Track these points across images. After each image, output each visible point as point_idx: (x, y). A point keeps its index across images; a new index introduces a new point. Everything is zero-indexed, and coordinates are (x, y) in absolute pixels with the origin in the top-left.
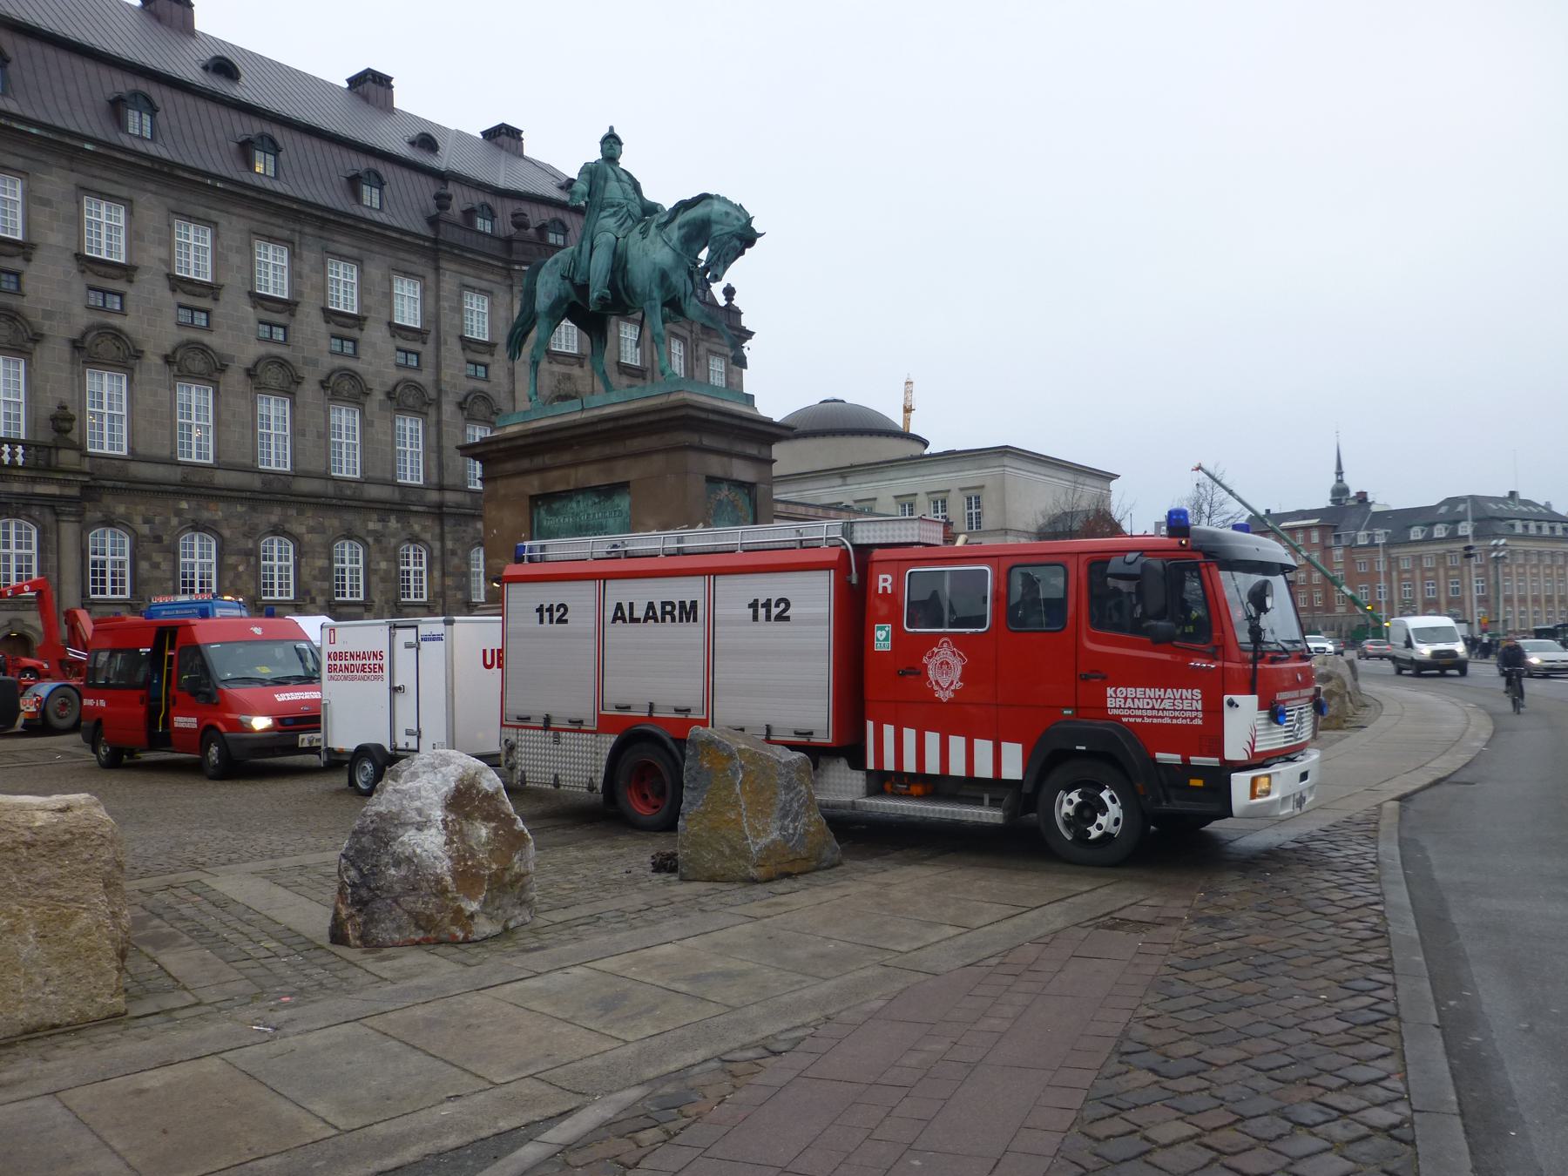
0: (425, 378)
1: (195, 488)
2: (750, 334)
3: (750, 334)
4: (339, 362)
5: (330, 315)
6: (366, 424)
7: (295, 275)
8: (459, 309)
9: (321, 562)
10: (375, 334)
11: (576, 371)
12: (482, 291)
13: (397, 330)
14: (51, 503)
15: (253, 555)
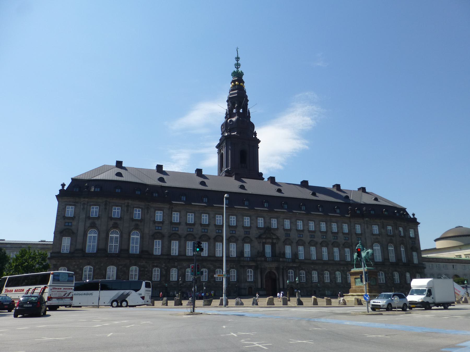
0: (349, 241)
1: (314, 263)
2: (419, 223)
3: (419, 223)
4: (334, 240)
5: (332, 233)
6: (340, 251)
7: (327, 227)
8: (355, 228)
9: (334, 276)
10: (340, 235)
11: (378, 237)
12: (359, 224)
13: (344, 234)
14: (295, 267)
15: (323, 275)
